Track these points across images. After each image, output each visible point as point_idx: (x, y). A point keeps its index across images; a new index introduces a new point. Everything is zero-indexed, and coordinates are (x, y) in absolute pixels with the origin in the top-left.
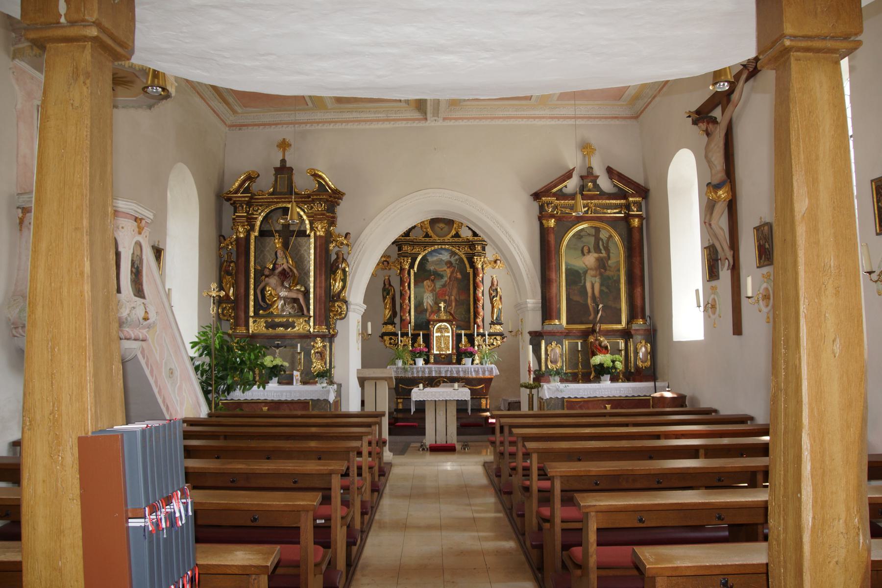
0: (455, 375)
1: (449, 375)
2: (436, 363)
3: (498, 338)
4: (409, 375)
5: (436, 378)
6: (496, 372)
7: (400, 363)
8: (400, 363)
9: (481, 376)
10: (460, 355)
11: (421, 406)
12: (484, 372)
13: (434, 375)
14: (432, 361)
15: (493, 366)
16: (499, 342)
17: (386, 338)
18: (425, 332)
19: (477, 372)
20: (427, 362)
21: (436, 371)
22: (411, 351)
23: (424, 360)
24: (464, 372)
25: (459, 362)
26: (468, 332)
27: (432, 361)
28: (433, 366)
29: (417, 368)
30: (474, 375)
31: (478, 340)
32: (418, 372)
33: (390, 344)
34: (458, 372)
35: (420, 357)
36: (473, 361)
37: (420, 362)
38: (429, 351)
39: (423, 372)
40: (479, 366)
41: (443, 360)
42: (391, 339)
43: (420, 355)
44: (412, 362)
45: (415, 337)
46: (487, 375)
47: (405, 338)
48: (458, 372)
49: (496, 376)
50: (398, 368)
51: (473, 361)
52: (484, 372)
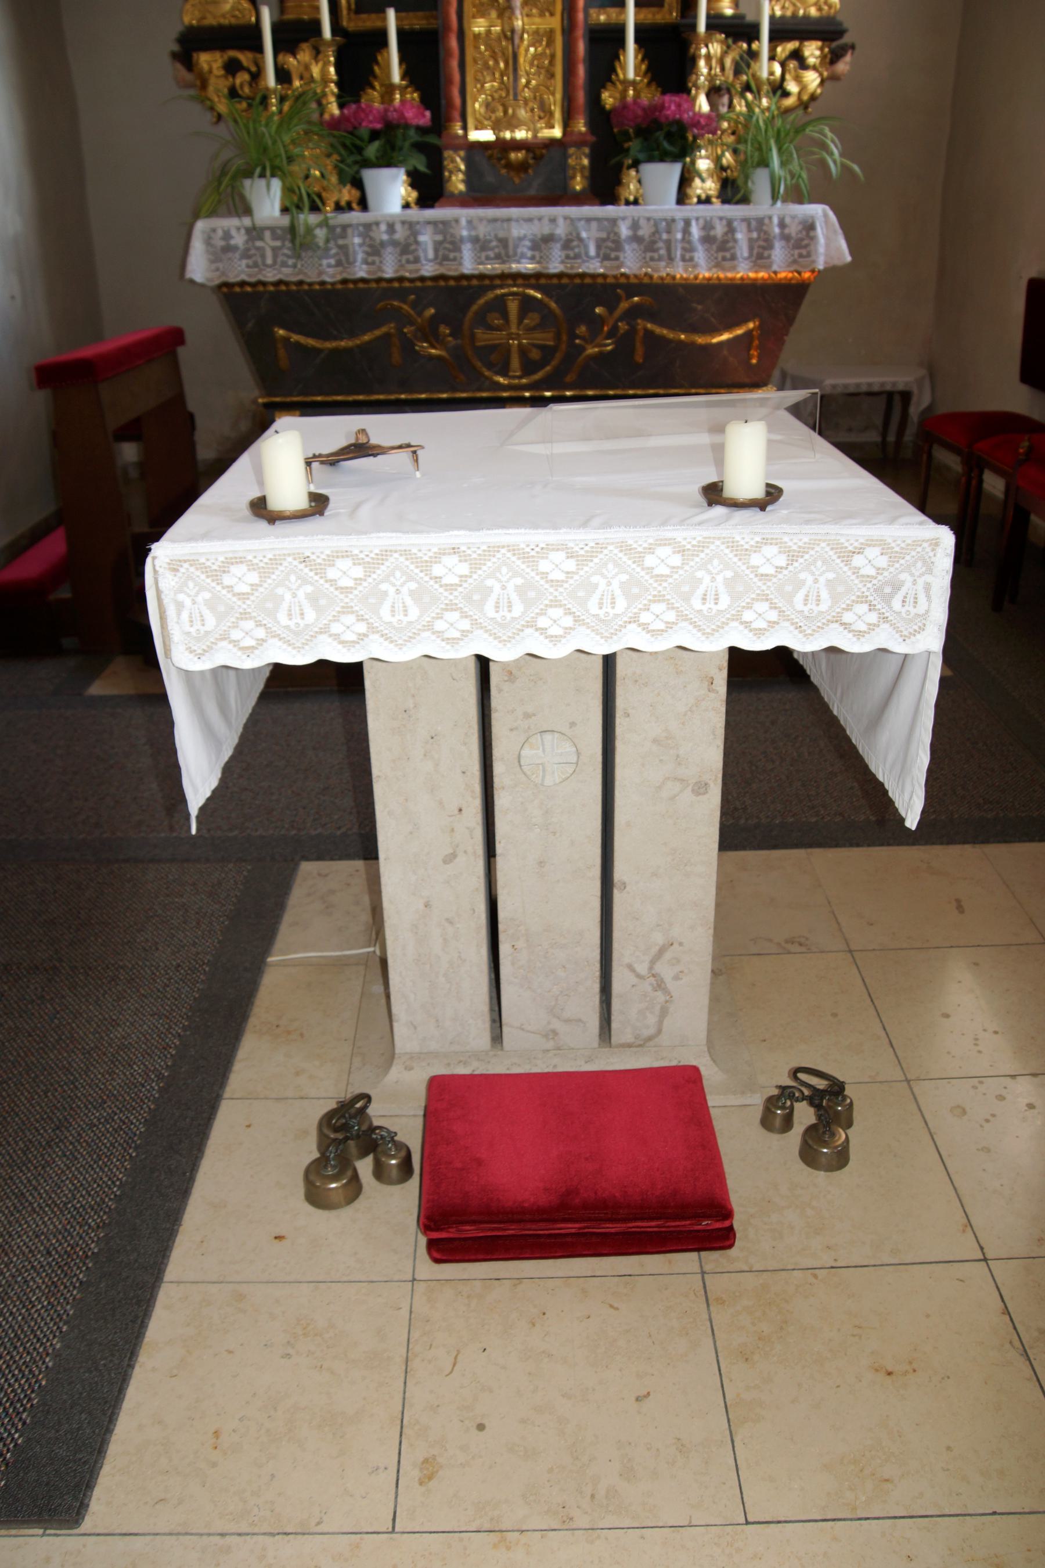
0: (596, 267)
1: (555, 267)
2: (480, 195)
3: (812, 51)
4: (326, 270)
5: (484, 282)
6: (831, 246)
7: (268, 201)
8: (268, 201)
9: (743, 271)
10: (613, 148)
11: (315, 706)
12: (760, 255)
13: (468, 264)
14: (458, 183)
15: (818, 211)
16: (812, 79)
17: (209, 61)
18: (418, 22)
19: (721, 246)
20: (429, 190)
21: (481, 245)
22: (335, 124)
23: (415, 180)
24: (648, 246)
25: (605, 189)
26: (652, 16)
27: (458, 183)
28: (464, 214)
29: (368, 227)
30: (704, 269)
31: (711, 56)
32: (375, 250)
33: (233, 93)
34: (609, 246)
35: (386, 161)
36: (685, 181)
37: (392, 191)
38: (439, 125)
39: (407, 249)
40: (718, 209)
41: (513, 176)
42: (232, 67)
43: (387, 143)
44: (347, 194)
45: (357, 58)
46: (780, 266)
47: (305, 55)
48: (609, 246)
49: (833, 271)
50: (255, 233)
51: (685, 181)
52: (760, 255)
